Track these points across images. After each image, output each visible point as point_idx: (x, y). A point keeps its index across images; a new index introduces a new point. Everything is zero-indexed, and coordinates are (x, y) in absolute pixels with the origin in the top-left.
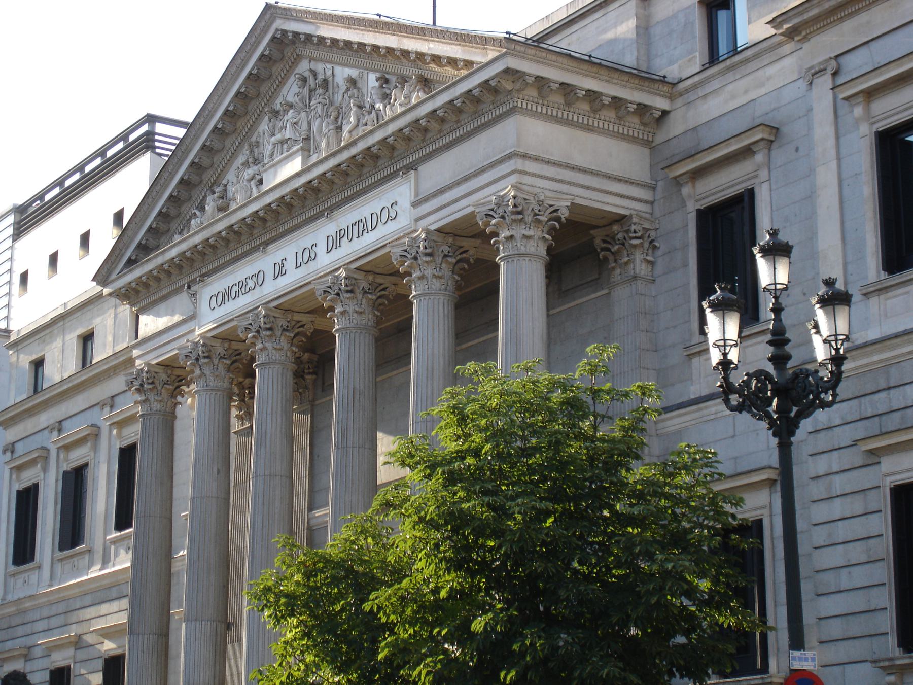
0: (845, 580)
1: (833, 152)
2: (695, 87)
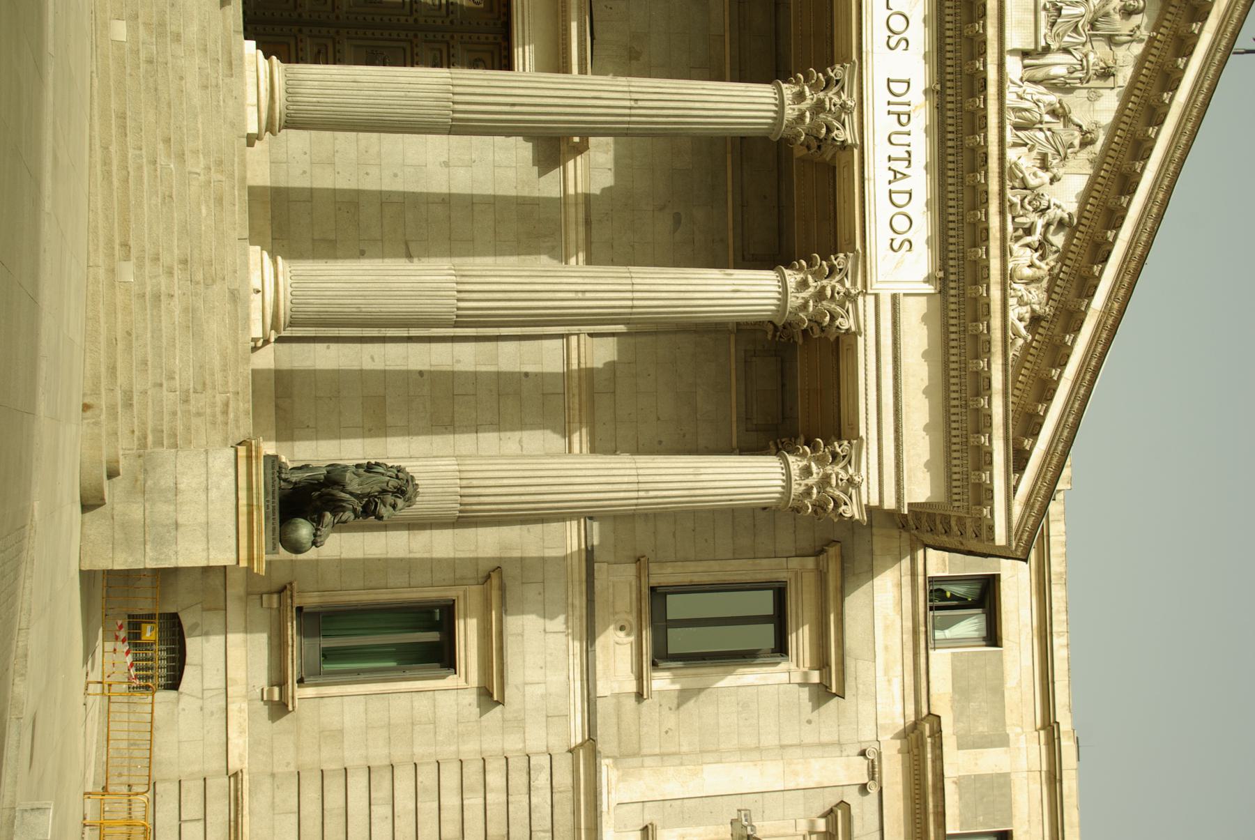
0: (381, 811)
1: (792, 786)
2: (913, 561)
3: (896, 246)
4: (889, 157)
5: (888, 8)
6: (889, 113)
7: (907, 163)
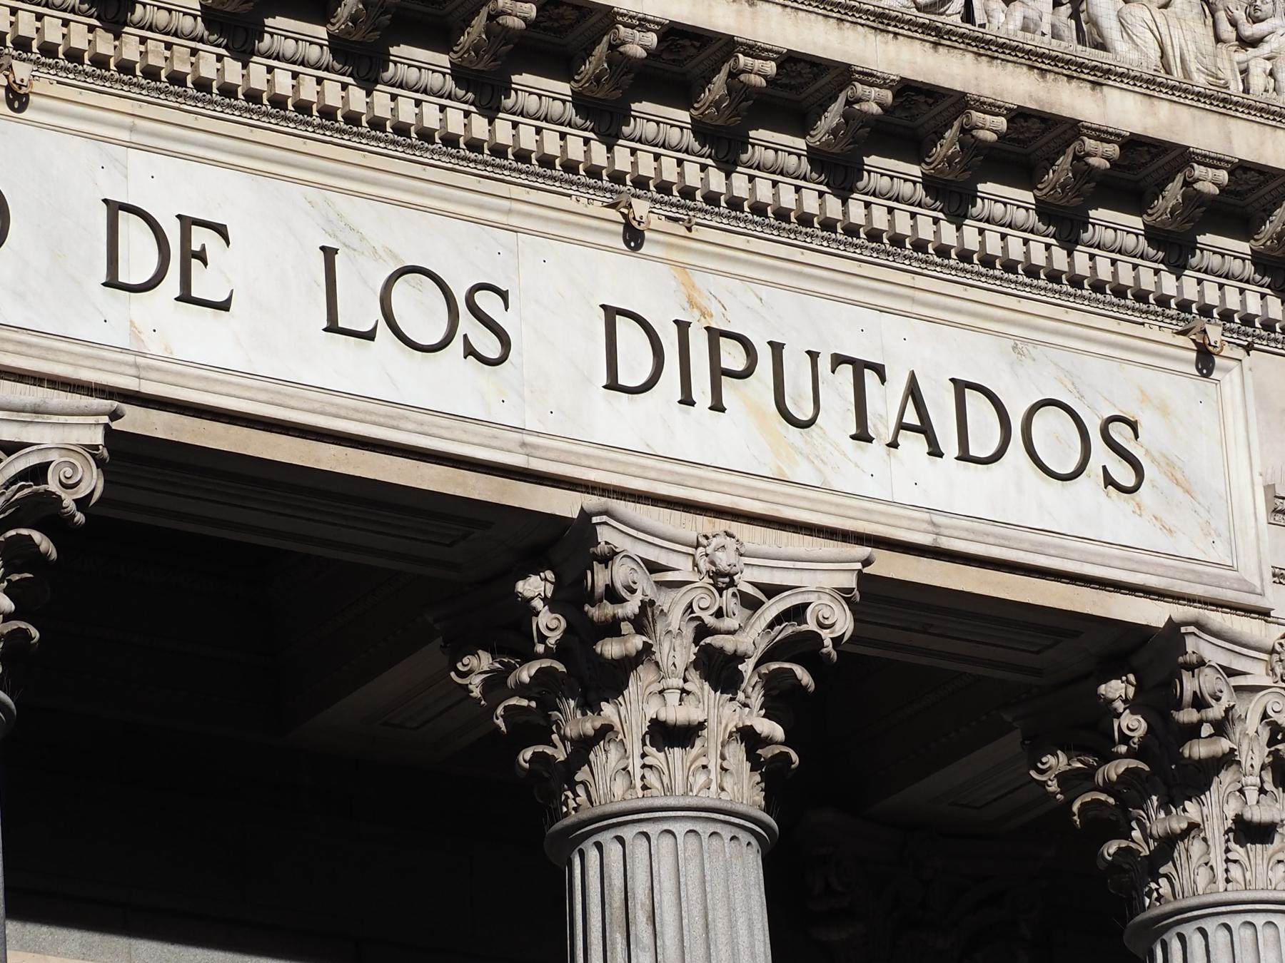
3: (1125, 475)
4: (888, 445)
5: (370, 336)
6: (718, 407)
7: (870, 377)
